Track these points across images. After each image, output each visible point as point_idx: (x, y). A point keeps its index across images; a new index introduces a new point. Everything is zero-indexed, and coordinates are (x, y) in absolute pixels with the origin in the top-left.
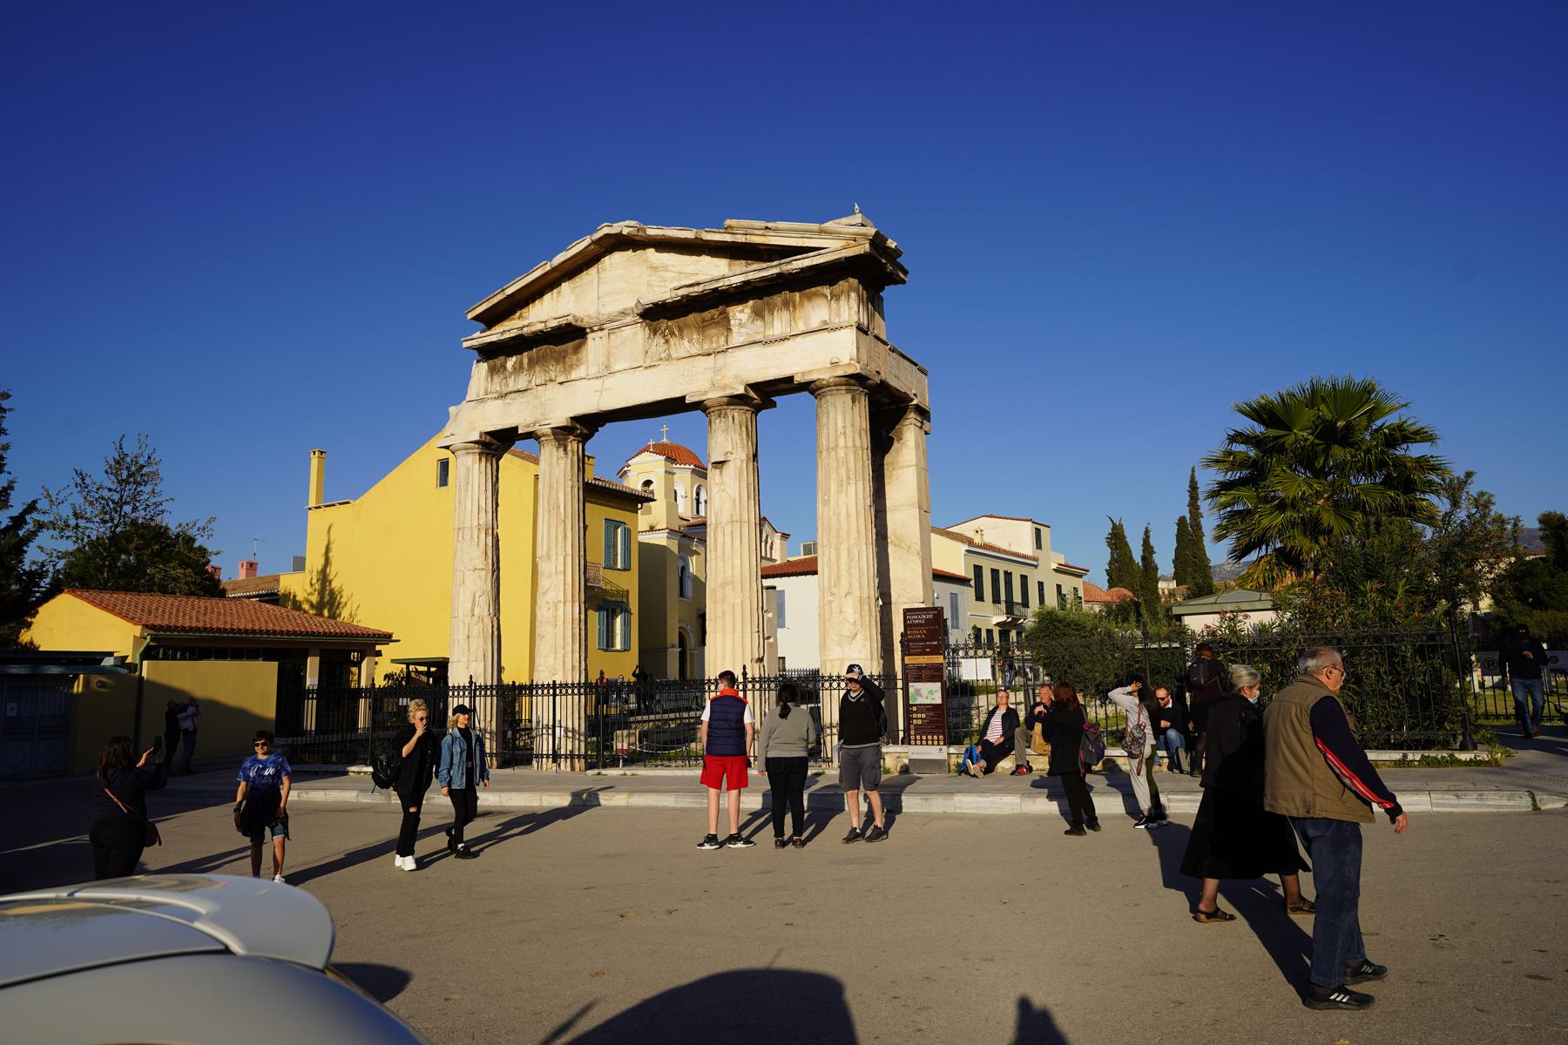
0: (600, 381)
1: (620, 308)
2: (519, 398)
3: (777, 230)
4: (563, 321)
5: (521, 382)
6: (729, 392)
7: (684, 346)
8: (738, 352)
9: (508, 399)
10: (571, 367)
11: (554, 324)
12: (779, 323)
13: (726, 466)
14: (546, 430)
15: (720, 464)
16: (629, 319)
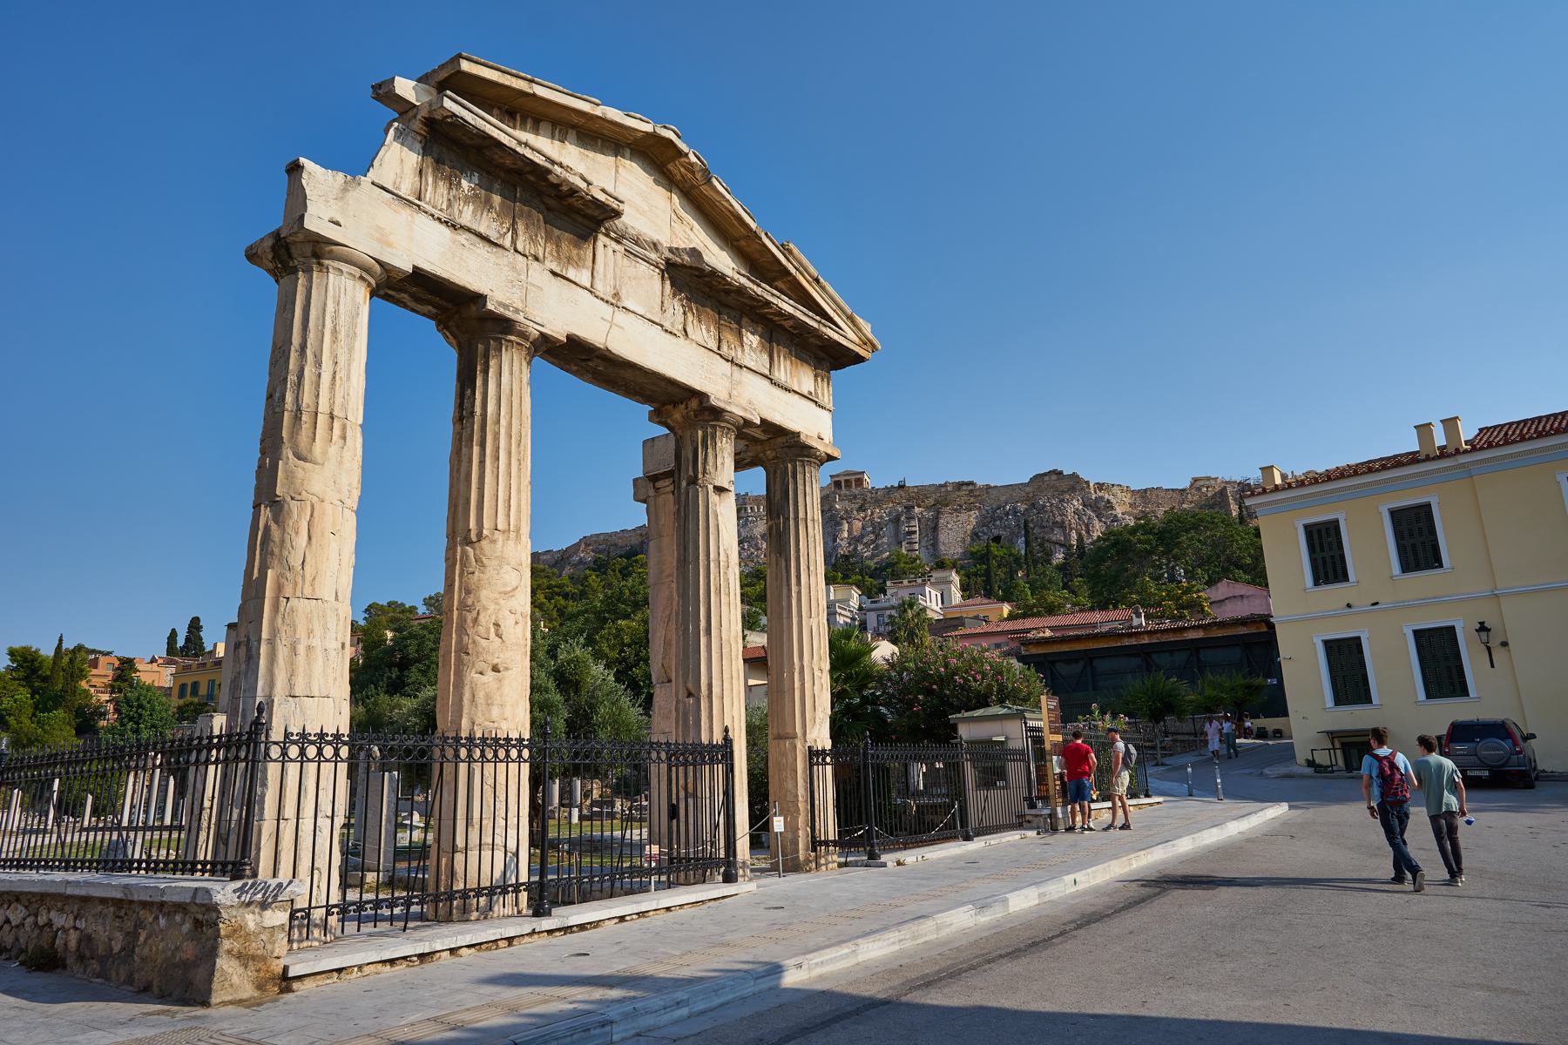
0: (610, 308)
1: (656, 237)
2: (483, 249)
3: (823, 288)
4: (614, 204)
5: (487, 225)
6: (748, 416)
7: (703, 332)
8: (751, 376)
9: (463, 237)
10: (569, 259)
11: (602, 197)
12: (785, 370)
13: (724, 495)
14: (533, 330)
15: (720, 490)
16: (653, 256)
